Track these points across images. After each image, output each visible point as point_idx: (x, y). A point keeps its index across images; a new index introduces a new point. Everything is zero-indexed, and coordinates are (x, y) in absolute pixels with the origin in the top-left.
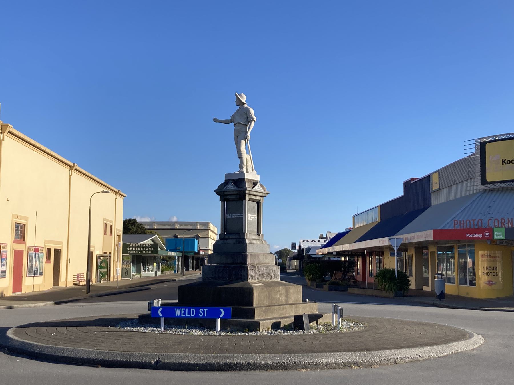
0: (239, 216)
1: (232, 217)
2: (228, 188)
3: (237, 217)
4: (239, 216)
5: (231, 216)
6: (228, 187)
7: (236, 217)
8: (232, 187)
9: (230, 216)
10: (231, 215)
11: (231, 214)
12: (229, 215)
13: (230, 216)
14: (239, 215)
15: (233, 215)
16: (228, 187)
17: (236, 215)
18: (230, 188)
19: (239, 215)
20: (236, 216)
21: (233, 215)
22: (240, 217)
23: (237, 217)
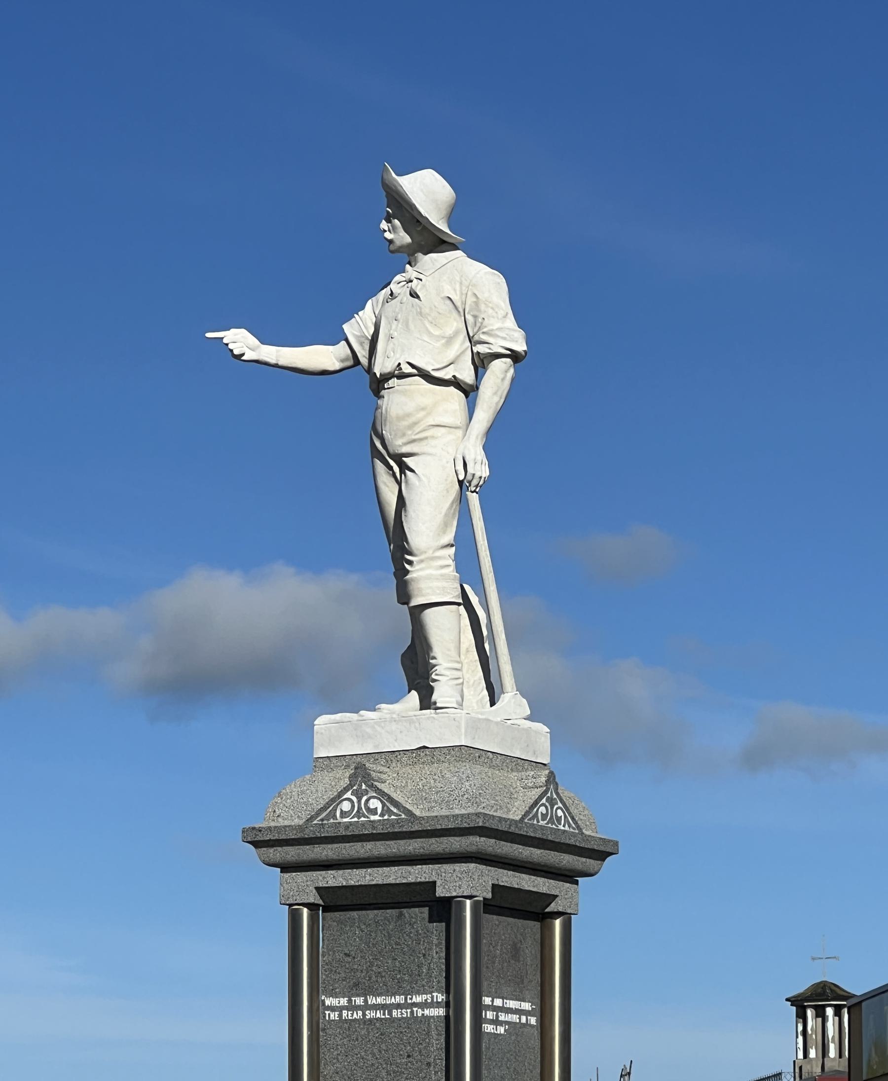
0: (424, 1005)
1: (370, 1014)
2: (344, 814)
3: (406, 1013)
4: (424, 1005)
5: (366, 1007)
6: (346, 806)
7: (395, 1013)
8: (374, 812)
9: (357, 1008)
10: (359, 1001)
11: (365, 996)
12: (344, 1001)
13: (357, 1008)
14: (418, 999)
15: (380, 1000)
16: (346, 806)
17: (399, 999)
18: (359, 814)
19: (418, 999)
20: (398, 1006)
21: (380, 1000)
22: (427, 1012)
23: (406, 1013)
